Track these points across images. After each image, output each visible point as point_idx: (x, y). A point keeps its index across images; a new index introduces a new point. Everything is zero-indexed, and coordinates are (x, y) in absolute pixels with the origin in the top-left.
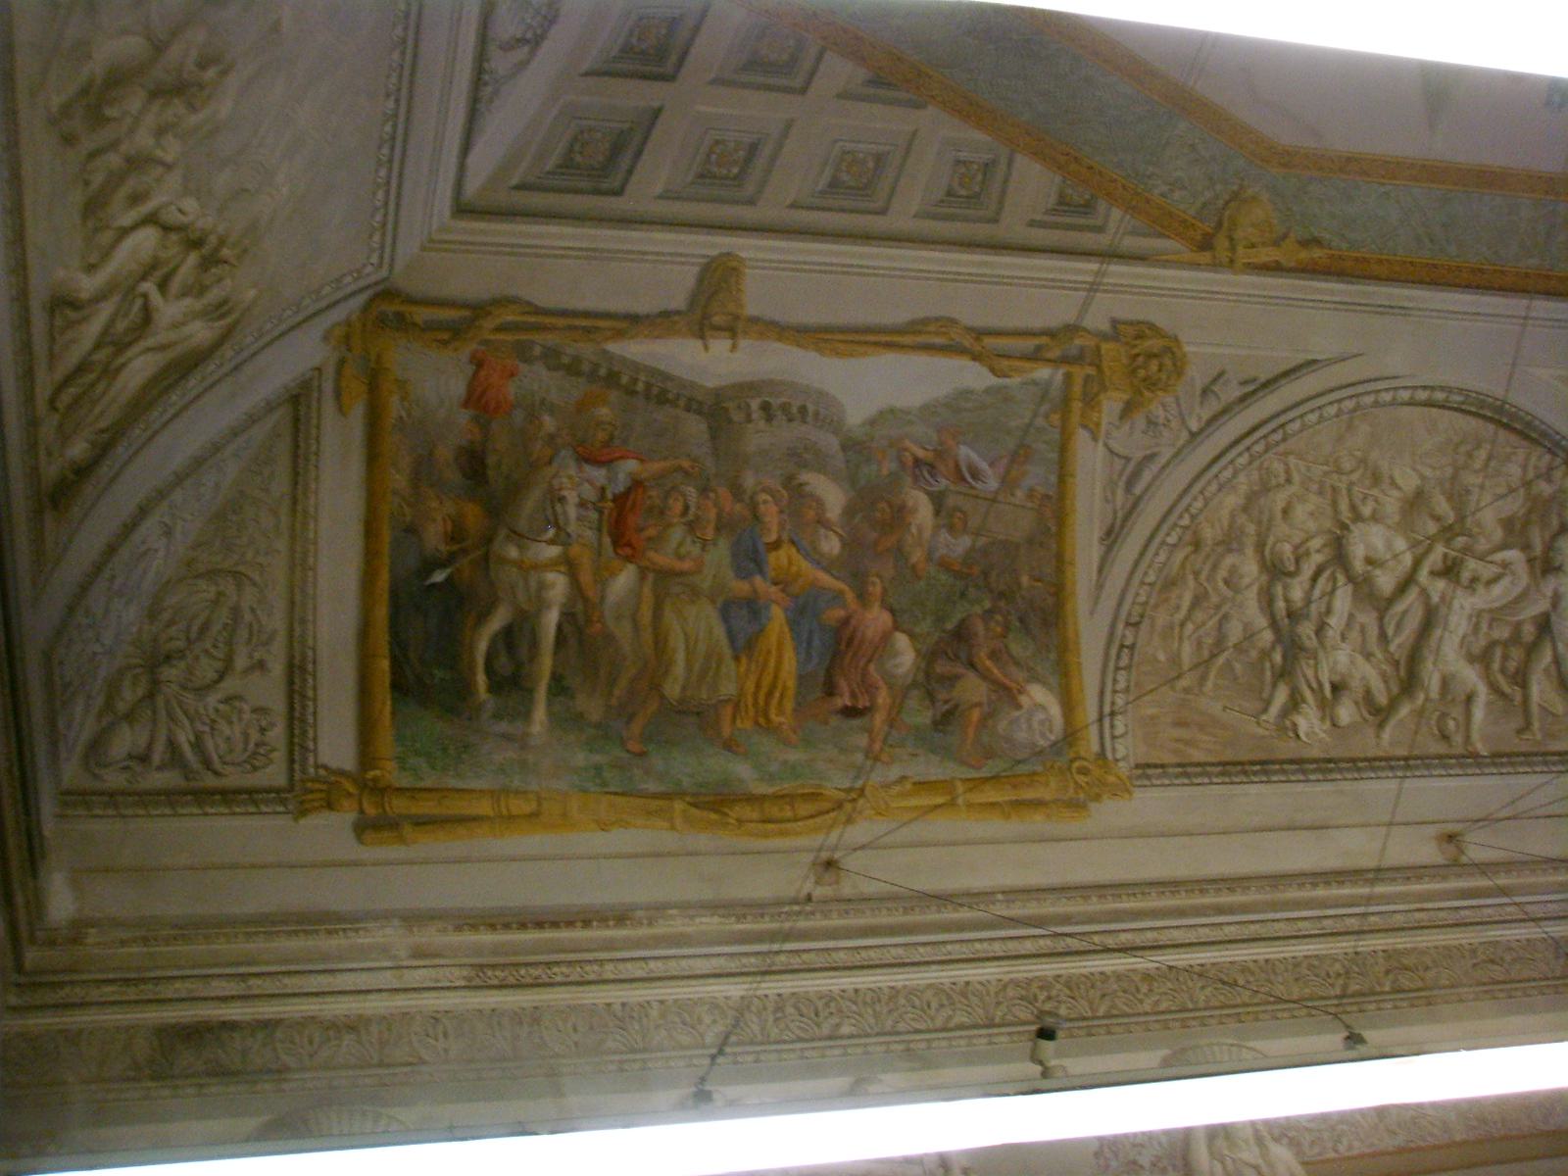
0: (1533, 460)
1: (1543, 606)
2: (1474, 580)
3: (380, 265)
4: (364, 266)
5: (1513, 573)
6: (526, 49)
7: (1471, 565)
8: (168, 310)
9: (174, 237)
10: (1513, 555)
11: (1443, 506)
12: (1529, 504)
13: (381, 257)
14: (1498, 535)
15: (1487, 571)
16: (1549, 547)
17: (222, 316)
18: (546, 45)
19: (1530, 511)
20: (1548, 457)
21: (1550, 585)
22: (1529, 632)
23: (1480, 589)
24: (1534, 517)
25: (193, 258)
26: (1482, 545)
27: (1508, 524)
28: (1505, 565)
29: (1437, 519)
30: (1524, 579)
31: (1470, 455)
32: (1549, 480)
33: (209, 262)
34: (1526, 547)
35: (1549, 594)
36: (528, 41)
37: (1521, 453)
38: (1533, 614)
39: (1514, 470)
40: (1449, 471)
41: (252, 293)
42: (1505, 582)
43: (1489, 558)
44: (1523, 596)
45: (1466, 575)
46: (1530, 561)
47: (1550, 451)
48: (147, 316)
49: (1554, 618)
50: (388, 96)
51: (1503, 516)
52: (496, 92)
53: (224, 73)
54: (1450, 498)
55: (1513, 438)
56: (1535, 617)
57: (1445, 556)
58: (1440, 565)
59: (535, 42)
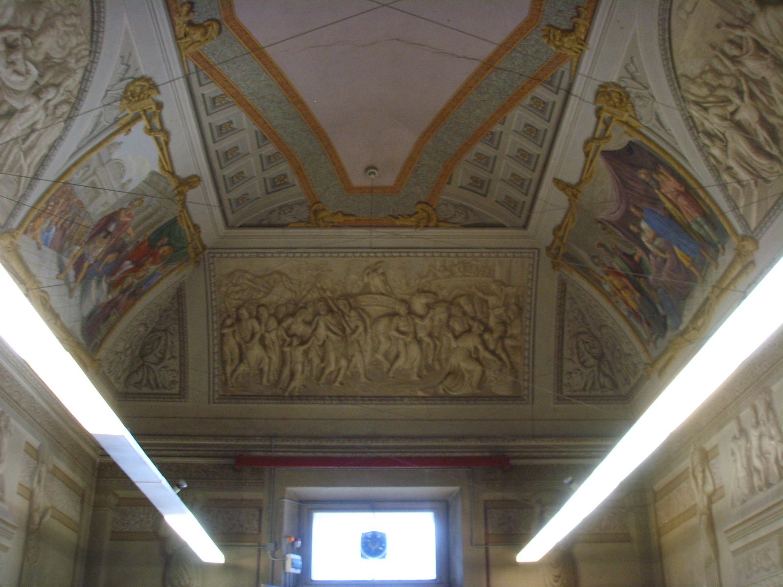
0: (83, 47)
1: (18, 105)
2: (13, 63)
5: (26, 79)
7: (18, 56)
10: (34, 72)
11: (39, 20)
12: (61, 61)
14: (40, 58)
15: (21, 67)
16: (46, 86)
19: (58, 64)
20: (87, 53)
21: (30, 101)
22: (5, 108)
23: (10, 70)
24: (57, 68)
26: (31, 54)
27: (48, 58)
28: (28, 72)
29: (33, 21)
30: (25, 87)
31: (71, 14)
32: (78, 61)
34: (41, 76)
35: (27, 102)
37: (83, 39)
38: (14, 105)
39: (74, 41)
40: (58, 9)
42: (21, 79)
43: (27, 62)
44: (17, 92)
45: (13, 57)
46: (36, 83)
47: (91, 52)
49: (17, 115)
51: (50, 53)
54: (45, 20)
55: (88, 30)
56: (12, 106)
57: (17, 39)
58: (10, 40)
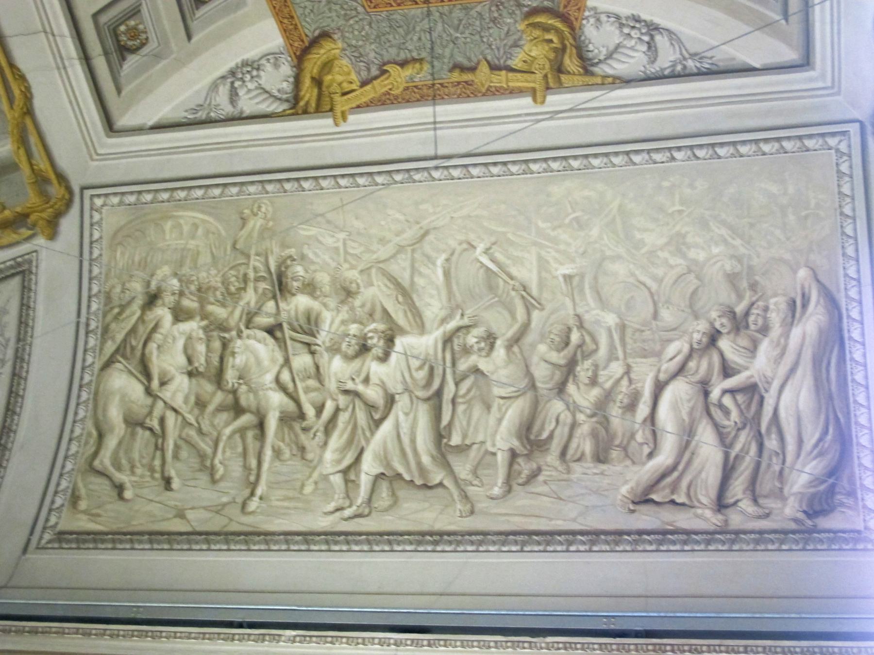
3: (843, 133)
4: (837, 150)
6: (658, 38)
8: (760, 365)
9: (692, 364)
13: (833, 134)
17: (805, 306)
18: (657, 20)
25: (724, 344)
33: (739, 323)
36: (652, 37)
41: (803, 273)
48: (751, 389)
50: (673, 159)
52: (693, 56)
53: (581, 326)
59: (653, 28)
